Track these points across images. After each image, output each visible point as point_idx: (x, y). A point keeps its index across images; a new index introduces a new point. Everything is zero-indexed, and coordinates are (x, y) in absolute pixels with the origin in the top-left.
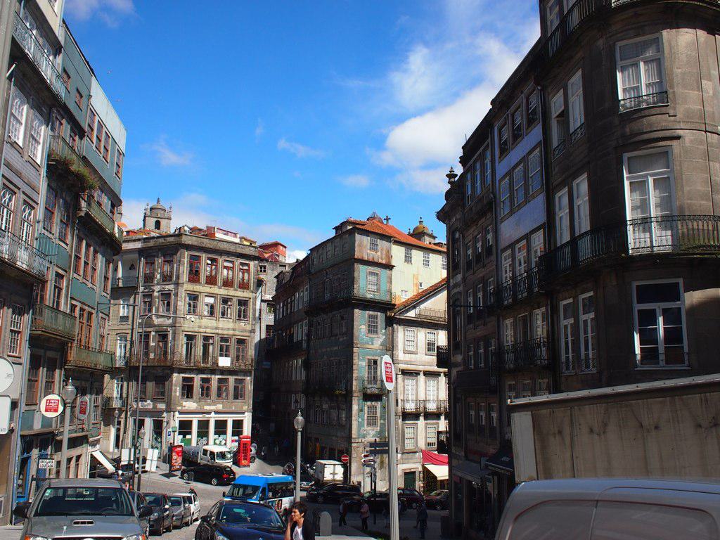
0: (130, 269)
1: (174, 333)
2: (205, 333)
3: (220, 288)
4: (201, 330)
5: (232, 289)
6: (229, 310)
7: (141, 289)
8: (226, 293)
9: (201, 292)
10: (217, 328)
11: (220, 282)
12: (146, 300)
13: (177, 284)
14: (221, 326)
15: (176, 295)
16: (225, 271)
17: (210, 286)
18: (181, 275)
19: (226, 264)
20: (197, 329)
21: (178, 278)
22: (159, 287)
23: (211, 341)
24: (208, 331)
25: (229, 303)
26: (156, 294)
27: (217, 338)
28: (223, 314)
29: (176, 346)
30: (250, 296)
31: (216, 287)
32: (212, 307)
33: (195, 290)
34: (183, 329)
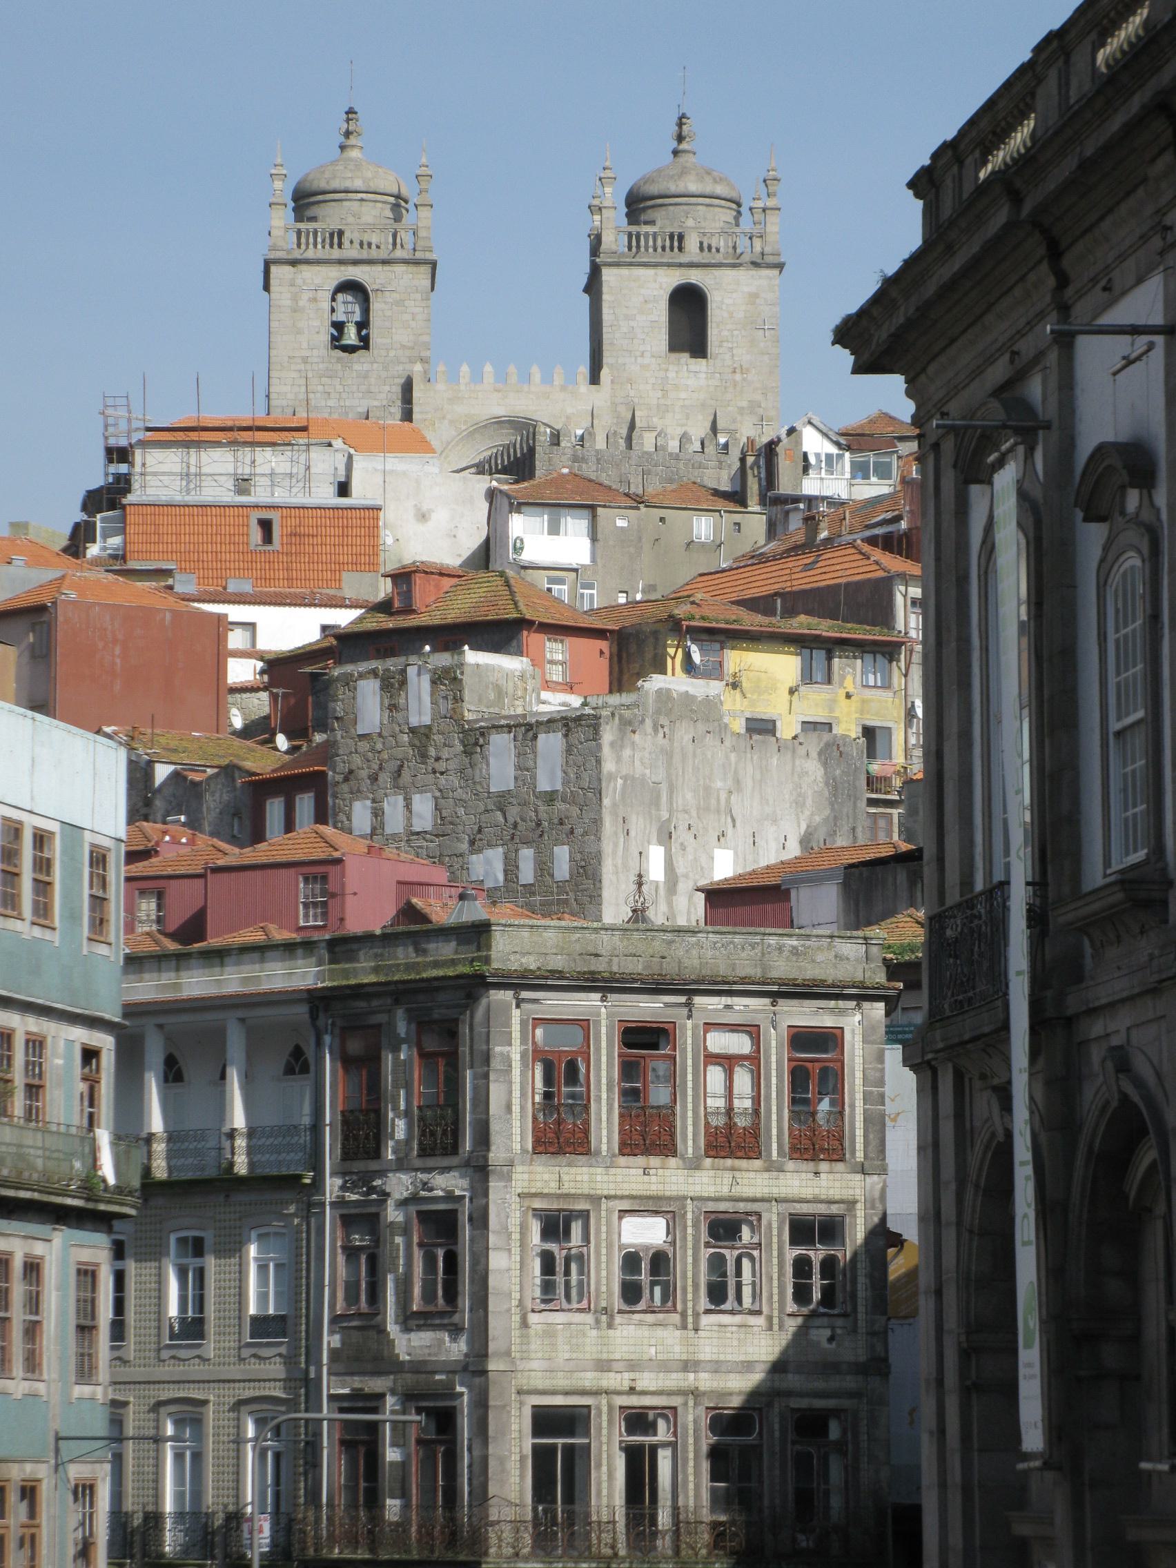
0: (289, 1071)
1: (481, 1404)
2: (632, 1391)
3: (694, 1165)
4: (612, 1380)
5: (757, 1163)
6: (746, 1263)
7: (332, 1186)
8: (725, 1191)
9: (596, 1199)
10: (688, 1366)
11: (690, 1137)
12: (357, 1240)
13: (480, 1171)
14: (707, 1349)
15: (481, 1220)
16: (715, 1076)
17: (640, 1160)
18: (495, 1126)
19: (719, 1042)
20: (588, 1379)
21: (483, 1138)
22: (405, 1178)
23: (663, 1432)
24: (647, 1381)
25: (746, 1232)
26: (393, 1214)
27: (694, 1419)
28: (717, 1294)
29: (492, 1463)
30: (846, 1194)
31: (672, 1162)
32: (660, 1261)
33: (568, 1188)
34: (522, 1381)
